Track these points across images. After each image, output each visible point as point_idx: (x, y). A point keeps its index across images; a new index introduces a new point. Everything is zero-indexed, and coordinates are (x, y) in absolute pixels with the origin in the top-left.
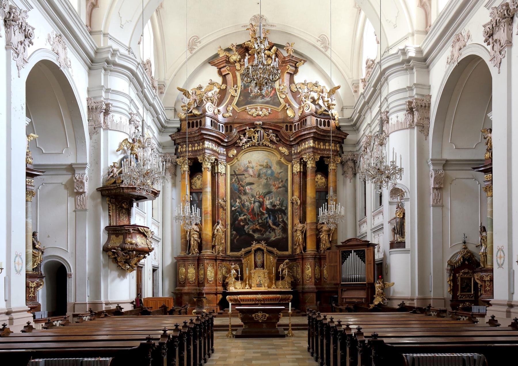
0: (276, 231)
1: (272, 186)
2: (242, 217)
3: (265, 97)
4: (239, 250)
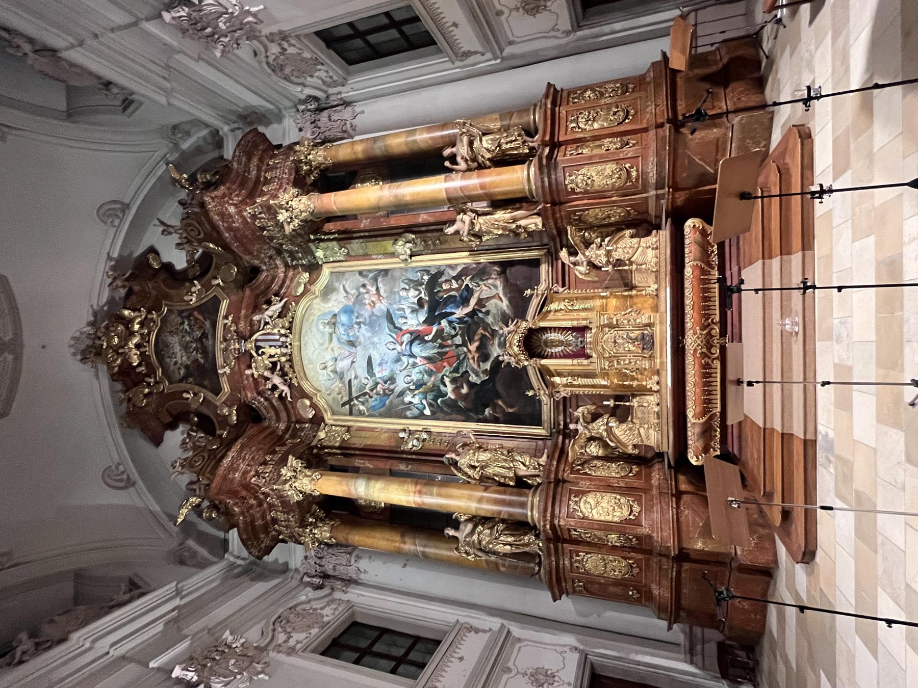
0: (483, 296)
1: (374, 310)
2: (449, 389)
3: (204, 331)
4: (535, 402)
